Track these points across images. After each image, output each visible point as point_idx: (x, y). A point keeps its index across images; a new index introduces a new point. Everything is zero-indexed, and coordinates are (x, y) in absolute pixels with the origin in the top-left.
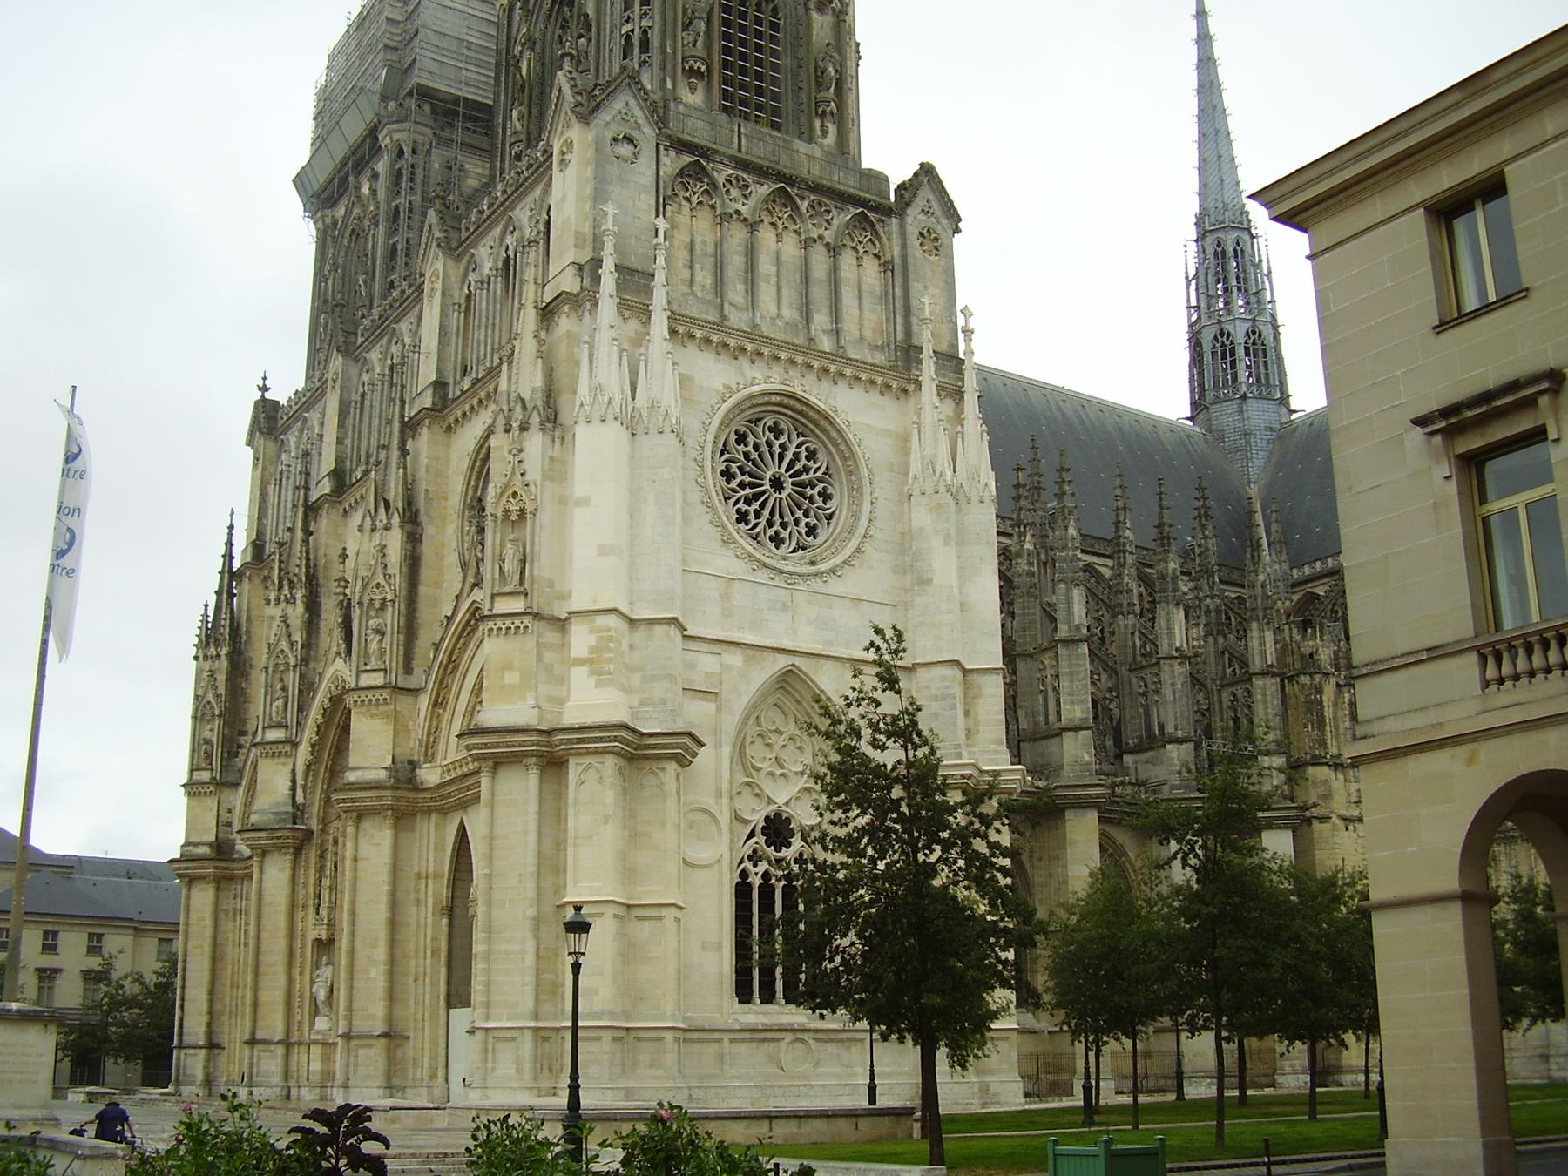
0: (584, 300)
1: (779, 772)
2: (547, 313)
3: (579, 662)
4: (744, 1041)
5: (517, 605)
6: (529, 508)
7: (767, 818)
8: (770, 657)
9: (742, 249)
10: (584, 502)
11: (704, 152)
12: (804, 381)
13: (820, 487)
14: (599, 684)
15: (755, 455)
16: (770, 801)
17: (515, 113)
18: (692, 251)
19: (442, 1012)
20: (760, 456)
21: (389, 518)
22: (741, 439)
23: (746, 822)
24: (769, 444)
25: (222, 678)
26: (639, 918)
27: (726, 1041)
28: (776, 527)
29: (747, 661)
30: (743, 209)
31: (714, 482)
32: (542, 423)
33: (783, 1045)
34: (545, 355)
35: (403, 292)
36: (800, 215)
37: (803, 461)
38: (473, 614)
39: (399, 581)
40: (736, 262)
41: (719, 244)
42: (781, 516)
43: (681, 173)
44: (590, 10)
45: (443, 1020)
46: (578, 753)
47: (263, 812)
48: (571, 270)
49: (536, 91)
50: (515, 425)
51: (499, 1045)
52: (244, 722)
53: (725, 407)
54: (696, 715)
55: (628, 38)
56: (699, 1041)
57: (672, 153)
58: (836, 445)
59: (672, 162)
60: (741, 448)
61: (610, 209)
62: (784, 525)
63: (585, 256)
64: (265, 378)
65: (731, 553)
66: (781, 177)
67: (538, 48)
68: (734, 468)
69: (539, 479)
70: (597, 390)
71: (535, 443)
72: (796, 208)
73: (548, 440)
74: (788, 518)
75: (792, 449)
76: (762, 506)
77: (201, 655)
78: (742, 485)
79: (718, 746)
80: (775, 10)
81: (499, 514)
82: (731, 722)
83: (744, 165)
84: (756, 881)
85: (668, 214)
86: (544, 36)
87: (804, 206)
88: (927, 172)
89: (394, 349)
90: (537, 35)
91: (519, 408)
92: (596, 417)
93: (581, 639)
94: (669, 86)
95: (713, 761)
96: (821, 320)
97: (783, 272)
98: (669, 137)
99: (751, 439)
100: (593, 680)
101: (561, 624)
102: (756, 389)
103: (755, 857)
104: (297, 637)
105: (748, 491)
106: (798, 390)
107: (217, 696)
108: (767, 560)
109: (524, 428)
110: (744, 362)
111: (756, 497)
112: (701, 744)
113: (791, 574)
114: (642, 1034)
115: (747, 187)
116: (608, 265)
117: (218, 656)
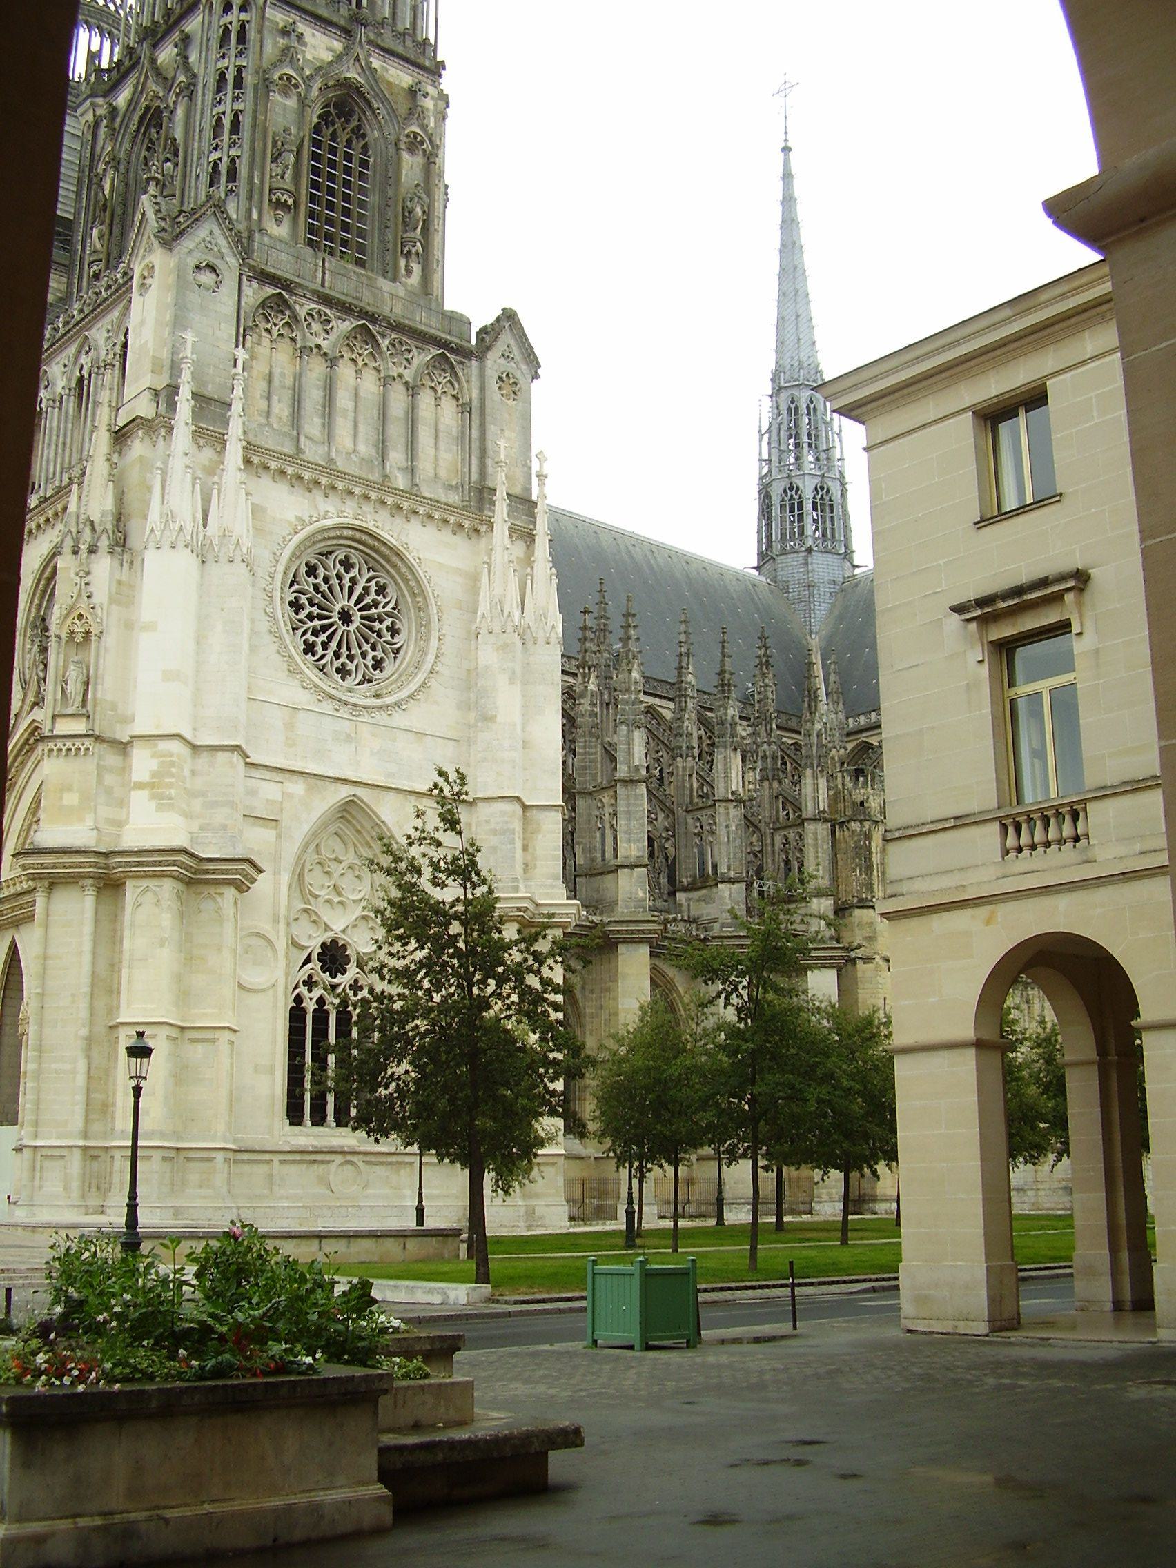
0: (158, 426)
1: (337, 899)
2: (120, 436)
3: (140, 786)
4: (294, 1162)
5: (79, 727)
6: (95, 630)
7: (323, 945)
8: (332, 786)
9: (321, 383)
10: (150, 627)
11: (286, 285)
12: (377, 517)
13: (388, 622)
14: (159, 808)
15: (324, 587)
16: (327, 928)
17: (95, 232)
18: (270, 382)
20: (330, 588)
22: (312, 571)
23: (303, 948)
24: (339, 577)
26: (193, 1041)
27: (276, 1163)
28: (343, 659)
30: (324, 344)
31: (283, 613)
32: (111, 547)
33: (333, 1167)
34: (117, 479)
36: (381, 353)
37: (373, 596)
38: (32, 734)
40: (313, 396)
41: (298, 377)
42: (349, 649)
43: (263, 305)
44: (178, 134)
46: (137, 876)
48: (147, 395)
49: (119, 210)
50: (83, 547)
51: (47, 1163)
53: (297, 539)
54: (256, 841)
55: (216, 166)
56: (249, 1161)
57: (255, 284)
58: (406, 581)
59: (254, 293)
60: (311, 580)
61: (189, 337)
62: (351, 658)
63: (161, 382)
65: (297, 683)
66: (363, 314)
67: (122, 168)
68: (303, 600)
69: (105, 601)
70: (168, 517)
71: (103, 566)
72: (377, 345)
73: (116, 564)
74: (356, 651)
75: (362, 583)
78: (311, 617)
79: (277, 873)
80: (365, 149)
81: (64, 635)
82: (291, 849)
83: (327, 300)
84: (310, 1006)
85: (248, 345)
86: (129, 156)
88: (509, 318)
90: (122, 155)
91: (88, 530)
92: (166, 545)
93: (142, 763)
94: (255, 216)
95: (271, 888)
96: (397, 457)
97: (361, 407)
98: (252, 268)
99: (321, 572)
100: (153, 804)
101: (123, 747)
102: (329, 523)
103: (310, 983)
105: (317, 623)
106: (371, 526)
108: (333, 692)
109: (92, 551)
110: (318, 495)
111: (324, 628)
112: (260, 871)
113: (356, 706)
114: (192, 1154)
115: (329, 321)
116: (185, 393)
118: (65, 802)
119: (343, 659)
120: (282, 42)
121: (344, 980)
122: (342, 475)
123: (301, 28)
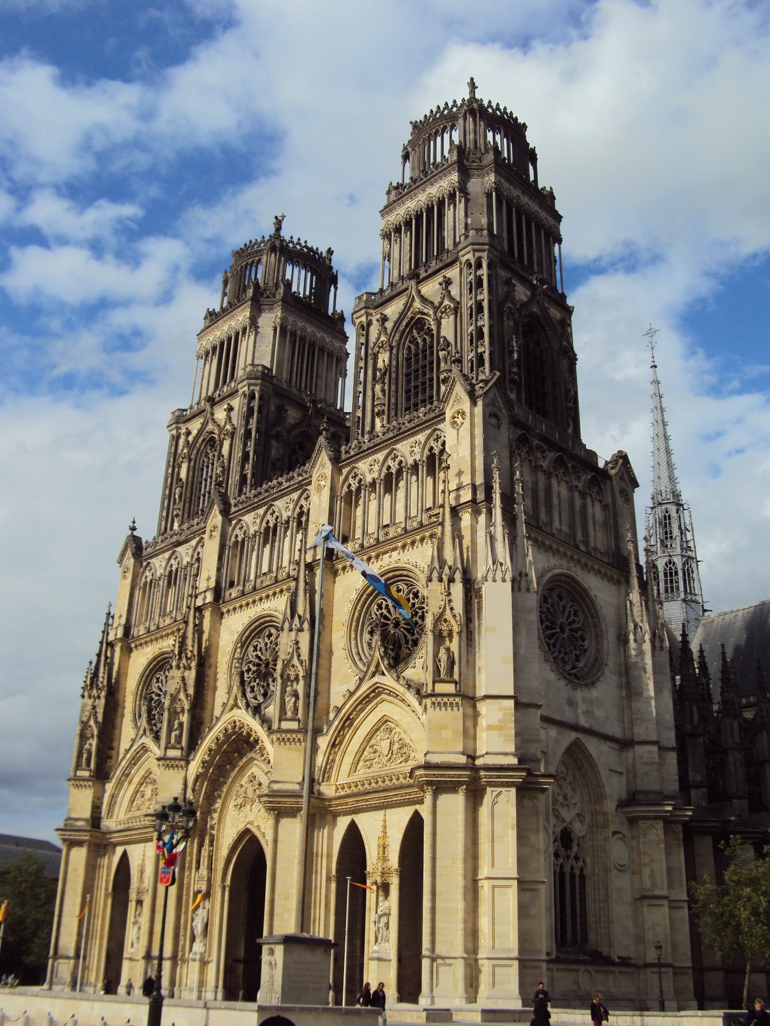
15: (552, 610)
16: (564, 821)
21: (302, 623)
24: (558, 605)
25: (100, 711)
35: (280, 484)
38: (374, 691)
40: (542, 494)
50: (445, 578)
52: (112, 741)
58: (589, 609)
62: (565, 653)
64: (134, 522)
65: (548, 668)
66: (560, 449)
67: (394, 351)
72: (566, 468)
76: (556, 640)
77: (86, 694)
89: (268, 517)
99: (550, 600)
104: (191, 691)
105: (550, 632)
107: (96, 722)
109: (451, 580)
111: (554, 634)
117: (99, 697)
119: (563, 655)
120: (506, 288)
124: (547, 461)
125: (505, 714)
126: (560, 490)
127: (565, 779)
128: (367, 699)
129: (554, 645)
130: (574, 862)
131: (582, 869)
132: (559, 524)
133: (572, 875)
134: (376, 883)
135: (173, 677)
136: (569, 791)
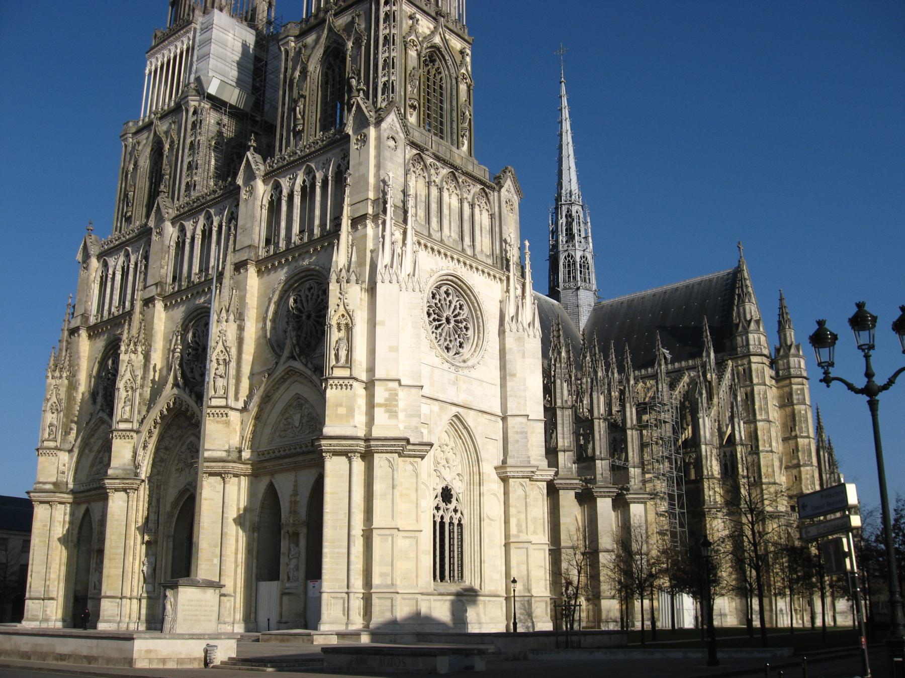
3: (380, 405)
13: (464, 323)
15: (439, 305)
19: (254, 583)
21: (228, 316)
22: (434, 297)
24: (445, 300)
29: (441, 408)
30: (437, 180)
39: (234, 351)
40: (434, 206)
45: (254, 588)
47: (116, 468)
57: (409, 147)
62: (451, 341)
83: (437, 158)
84: (438, 520)
87: (460, 180)
99: (438, 297)
100: (387, 415)
103: (437, 508)
105: (437, 323)
106: (459, 274)
111: (440, 325)
117: (61, 377)
118: (339, 412)
119: (448, 342)
121: (451, 506)
122: (448, 247)
123: (418, 16)
124: (440, 177)
125: (391, 394)
126: (451, 200)
127: (447, 445)
128: (283, 380)
129: (441, 335)
130: (453, 513)
131: (460, 521)
132: (450, 232)
133: (451, 523)
134: (288, 532)
135: (123, 361)
136: (450, 455)
